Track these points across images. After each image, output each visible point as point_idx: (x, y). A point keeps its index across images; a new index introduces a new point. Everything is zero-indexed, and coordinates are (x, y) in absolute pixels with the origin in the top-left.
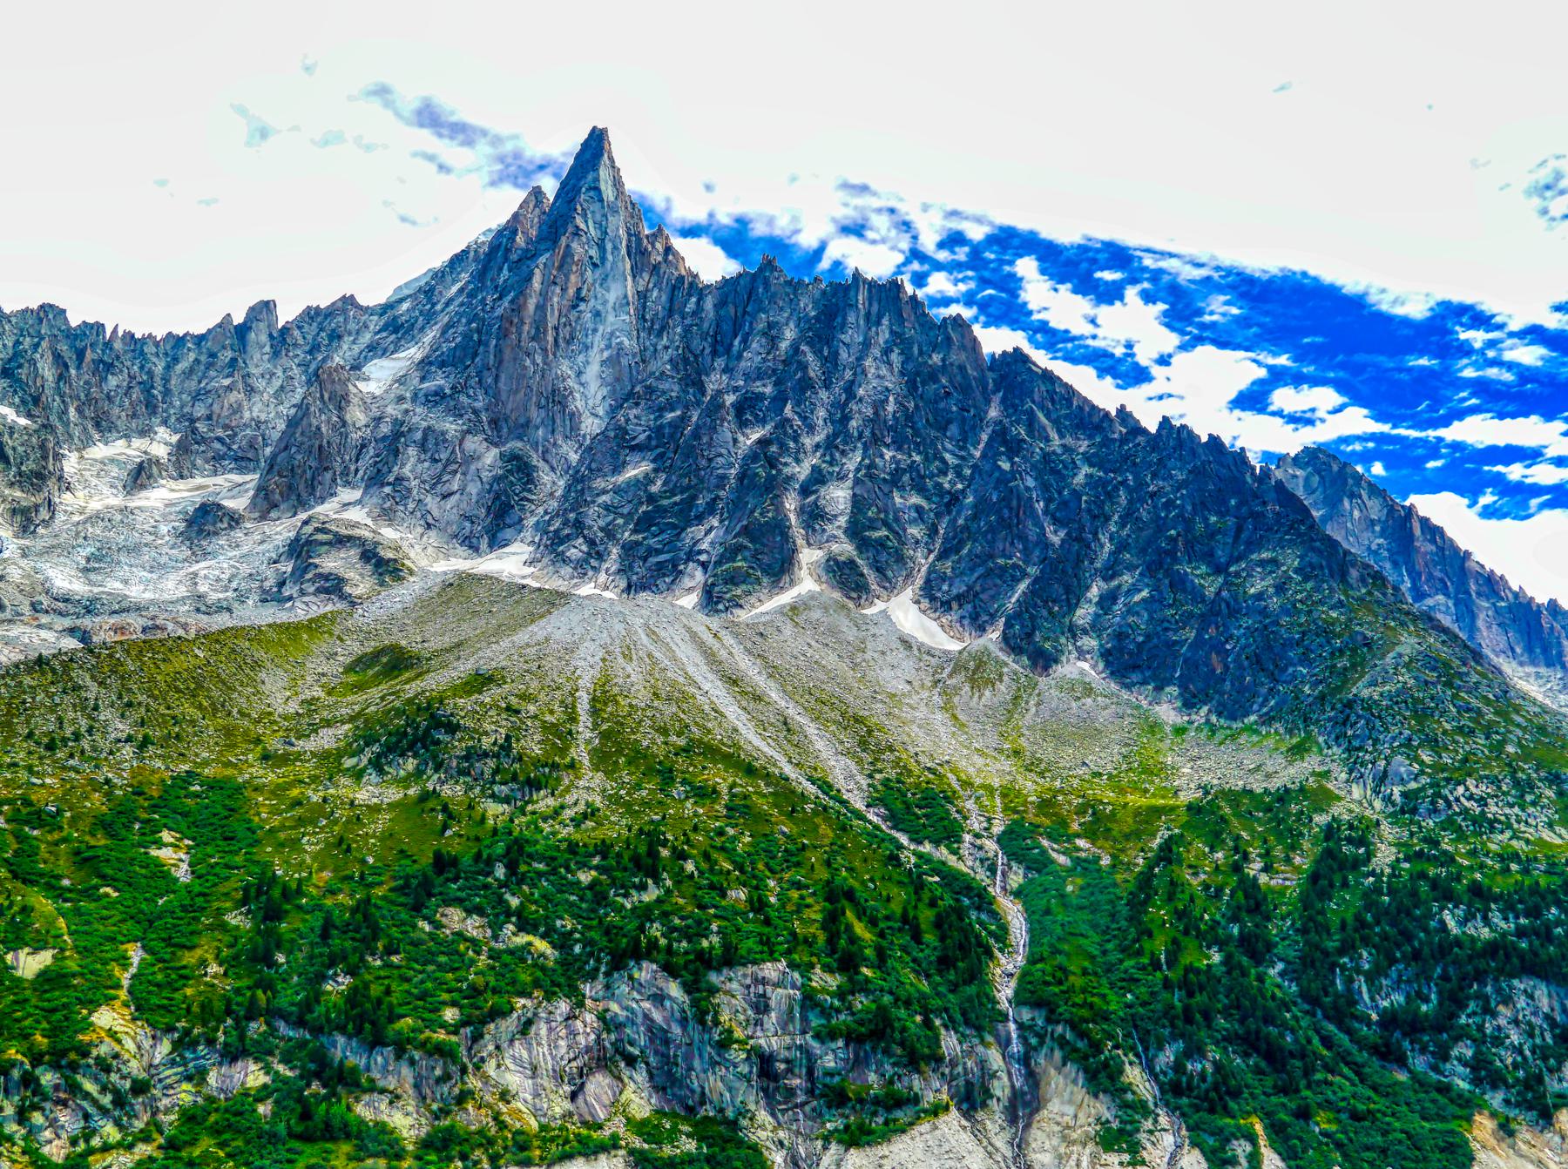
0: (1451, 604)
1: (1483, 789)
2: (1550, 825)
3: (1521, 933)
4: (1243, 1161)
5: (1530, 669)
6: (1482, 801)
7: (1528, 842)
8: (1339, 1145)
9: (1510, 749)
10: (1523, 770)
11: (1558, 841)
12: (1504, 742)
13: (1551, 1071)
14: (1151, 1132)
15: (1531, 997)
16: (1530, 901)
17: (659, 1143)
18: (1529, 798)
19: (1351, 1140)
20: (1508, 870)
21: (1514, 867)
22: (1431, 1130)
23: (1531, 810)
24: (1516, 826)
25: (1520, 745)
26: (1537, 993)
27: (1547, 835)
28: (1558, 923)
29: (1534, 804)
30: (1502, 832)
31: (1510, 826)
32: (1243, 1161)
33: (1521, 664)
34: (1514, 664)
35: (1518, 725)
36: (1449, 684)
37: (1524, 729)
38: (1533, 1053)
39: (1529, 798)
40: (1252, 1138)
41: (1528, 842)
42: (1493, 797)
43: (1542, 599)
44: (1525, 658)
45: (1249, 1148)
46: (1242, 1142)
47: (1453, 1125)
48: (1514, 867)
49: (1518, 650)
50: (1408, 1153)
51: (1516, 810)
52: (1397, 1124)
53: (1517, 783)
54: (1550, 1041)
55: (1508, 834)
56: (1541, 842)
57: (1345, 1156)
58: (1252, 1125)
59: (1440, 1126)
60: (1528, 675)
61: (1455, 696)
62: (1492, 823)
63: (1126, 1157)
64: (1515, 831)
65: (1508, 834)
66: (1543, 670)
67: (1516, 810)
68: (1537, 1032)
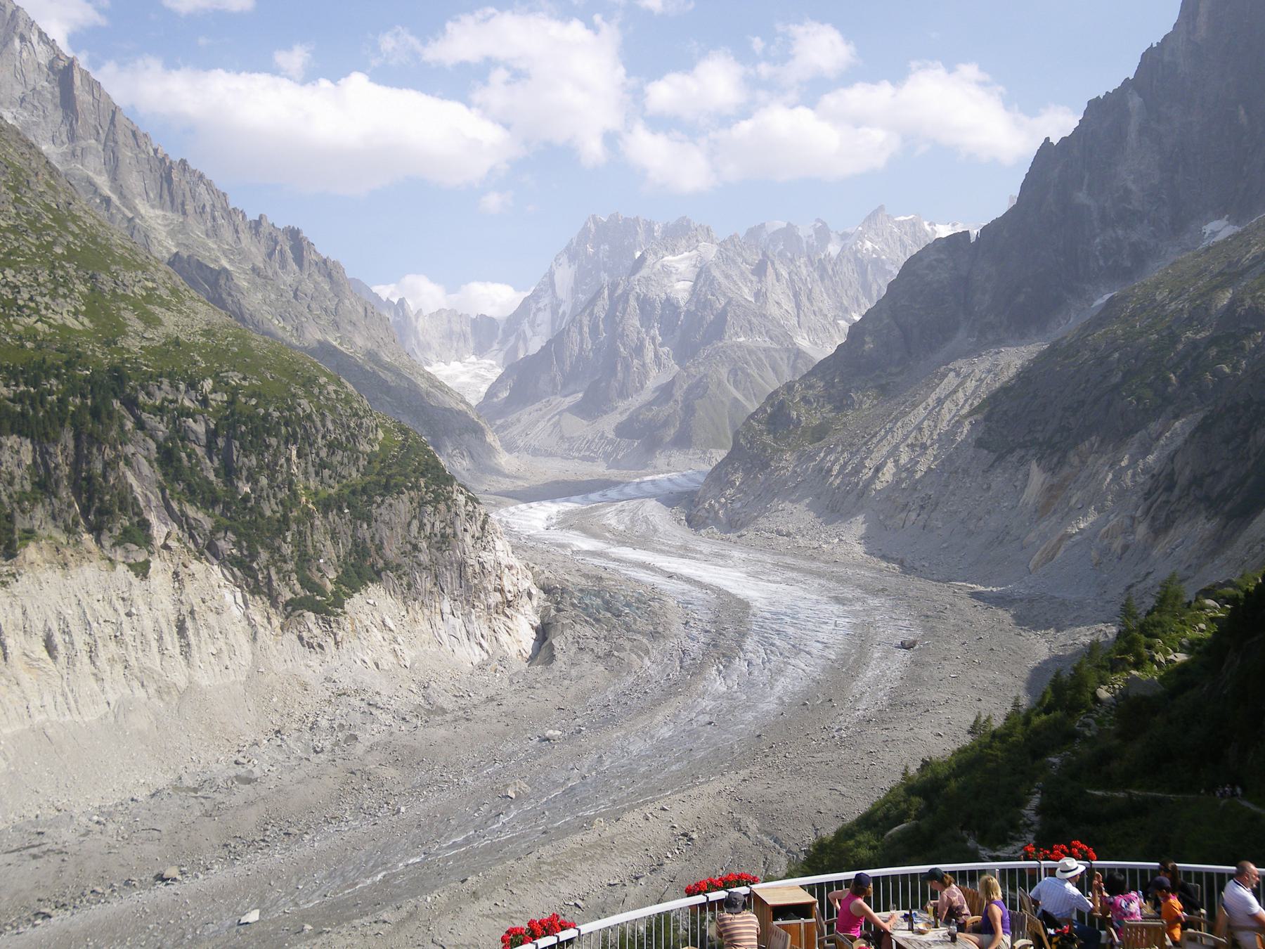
0: (100, 148)
1: (21, 279)
2: (76, 314)
3: (18, 399)
5: (159, 212)
6: (15, 289)
7: (50, 326)
9: (58, 250)
10: (63, 267)
11: (81, 328)
12: (54, 243)
13: (23, 511)
15: (18, 452)
16: (34, 372)
18: (61, 291)
20: (22, 346)
21: (29, 345)
23: (61, 300)
24: (43, 312)
25: (68, 247)
26: (23, 449)
27: (71, 322)
28: (51, 393)
29: (65, 296)
30: (29, 316)
31: (37, 311)
33: (153, 207)
34: (147, 206)
35: (72, 233)
36: (15, 189)
37: (75, 236)
38: (10, 497)
39: (61, 291)
41: (50, 326)
42: (27, 287)
43: (175, 157)
44: (156, 203)
48: (29, 345)
49: (152, 195)
51: (47, 299)
53: (54, 280)
54: (28, 487)
55: (34, 318)
56: (64, 328)
60: (157, 217)
61: (17, 199)
62: (20, 308)
64: (41, 316)
65: (34, 318)
66: (169, 214)
67: (47, 299)
68: (17, 480)
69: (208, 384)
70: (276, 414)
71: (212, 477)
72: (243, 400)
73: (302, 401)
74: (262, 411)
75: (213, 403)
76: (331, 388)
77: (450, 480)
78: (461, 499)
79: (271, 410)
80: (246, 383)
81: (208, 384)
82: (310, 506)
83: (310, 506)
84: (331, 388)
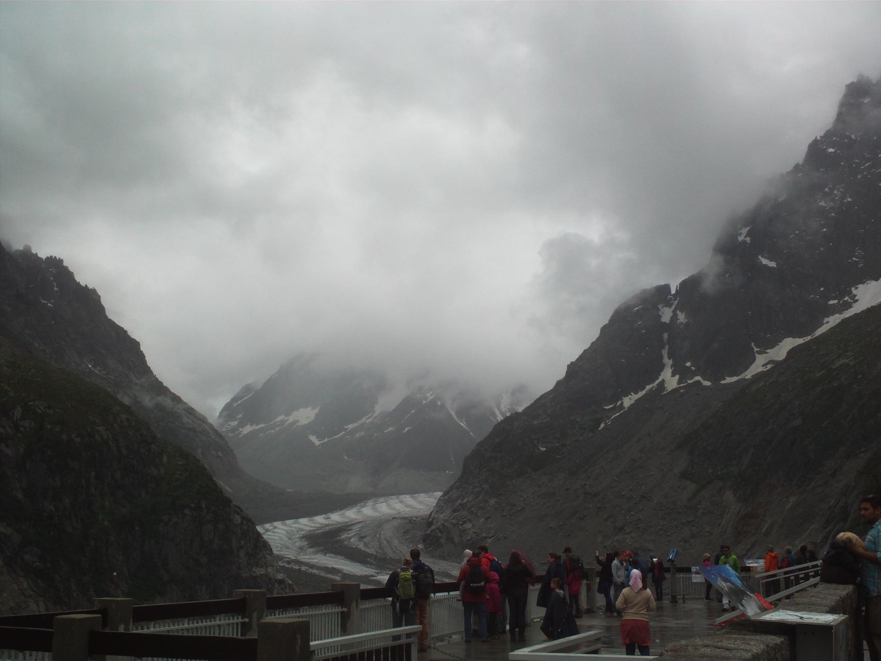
69: (18, 413)
70: (78, 440)
71: (20, 496)
72: (49, 427)
73: (100, 428)
74: (64, 437)
75: (22, 429)
76: (124, 416)
77: (227, 501)
78: (238, 519)
79: (73, 436)
80: (51, 412)
81: (18, 413)
82: (106, 523)
83: (106, 523)
84: (124, 416)
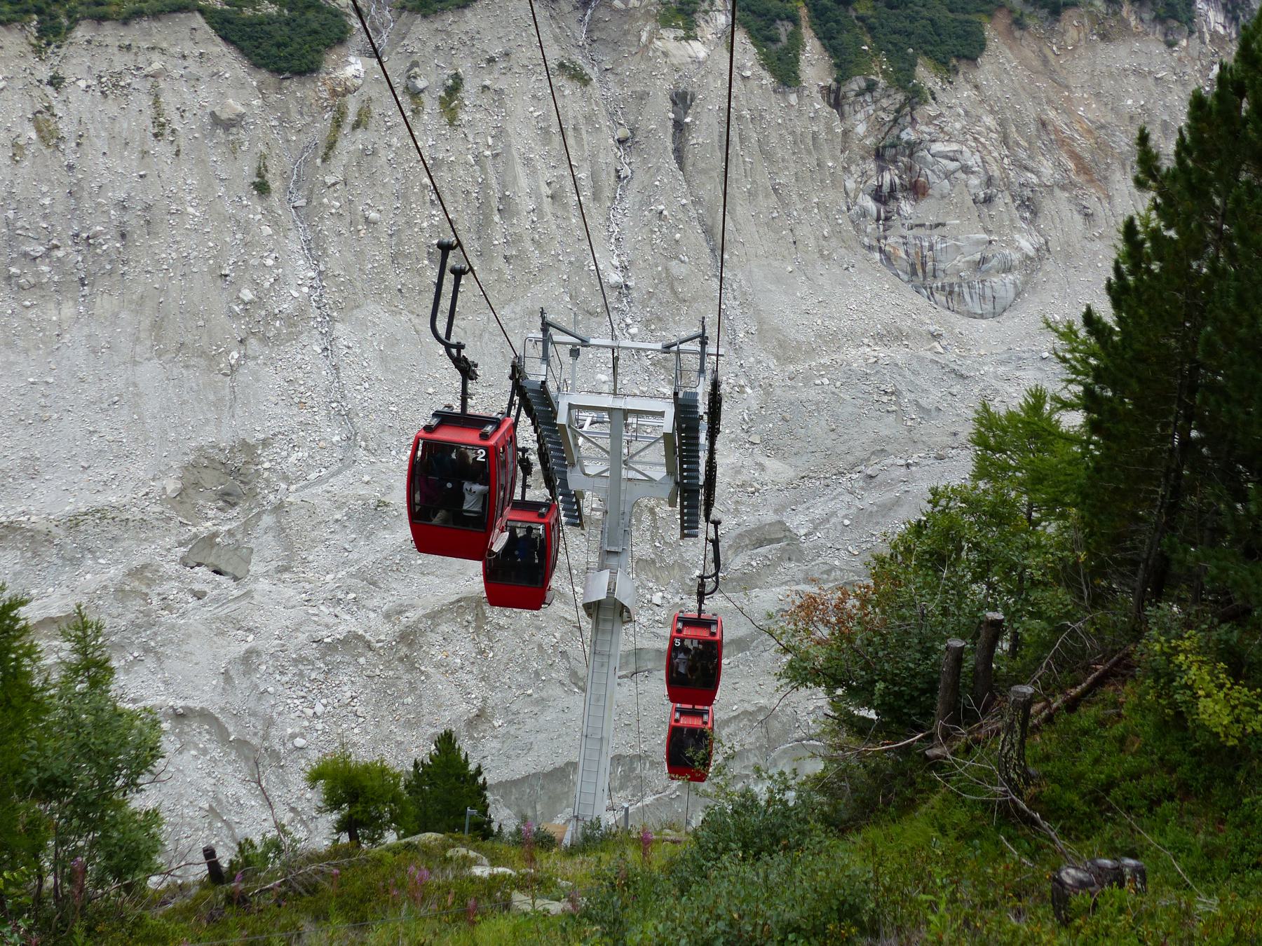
4: (784, 38)
8: (871, 29)
14: (706, 12)
17: (240, 7)
19: (882, 25)
22: (954, 20)
32: (784, 38)
40: (794, 20)
45: (790, 27)
46: (785, 23)
47: (972, 17)
50: (929, 36)
52: (925, 13)
57: (873, 37)
58: (797, 9)
59: (961, 17)
63: (681, 33)
